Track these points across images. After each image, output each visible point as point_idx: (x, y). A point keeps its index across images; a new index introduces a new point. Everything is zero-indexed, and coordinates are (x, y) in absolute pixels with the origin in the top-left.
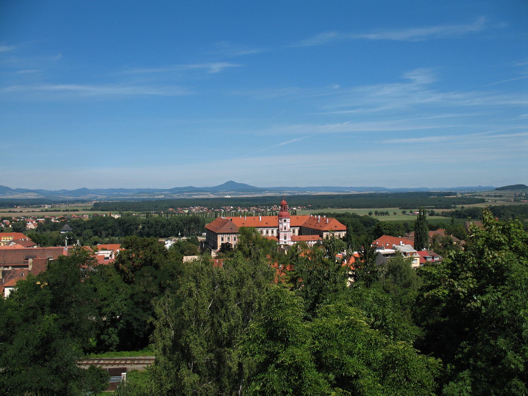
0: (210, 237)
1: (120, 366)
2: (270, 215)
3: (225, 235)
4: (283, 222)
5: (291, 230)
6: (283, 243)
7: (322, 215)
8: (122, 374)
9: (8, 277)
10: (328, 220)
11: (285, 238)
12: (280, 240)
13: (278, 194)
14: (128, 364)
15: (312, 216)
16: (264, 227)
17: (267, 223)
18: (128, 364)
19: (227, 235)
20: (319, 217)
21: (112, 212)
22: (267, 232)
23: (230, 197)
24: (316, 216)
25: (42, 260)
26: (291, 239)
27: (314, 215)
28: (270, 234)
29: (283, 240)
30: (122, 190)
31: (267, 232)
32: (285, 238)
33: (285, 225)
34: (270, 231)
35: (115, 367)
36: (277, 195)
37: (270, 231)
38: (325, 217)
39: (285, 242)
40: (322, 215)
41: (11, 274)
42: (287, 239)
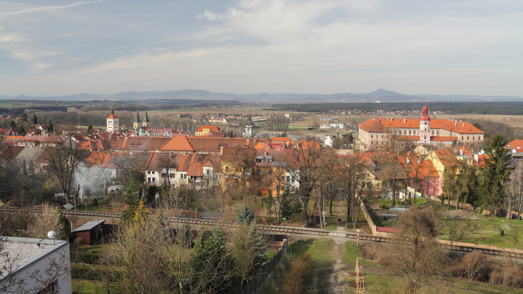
0: (362, 135)
1: (284, 234)
2: (413, 119)
5: (431, 131)
6: (424, 142)
7: (459, 120)
8: (284, 240)
9: (206, 159)
10: (463, 124)
11: (425, 138)
12: (420, 139)
13: (421, 101)
14: (289, 232)
16: (408, 128)
17: (410, 125)
18: (289, 232)
19: (376, 134)
20: (456, 121)
21: (285, 112)
22: (410, 132)
23: (380, 102)
24: (453, 121)
25: (230, 147)
27: (451, 119)
28: (412, 134)
29: (423, 139)
30: (294, 95)
31: (410, 132)
32: (425, 138)
34: (412, 132)
35: (279, 233)
36: (420, 102)
37: (412, 132)
38: (461, 121)
41: (208, 157)
42: (427, 139)
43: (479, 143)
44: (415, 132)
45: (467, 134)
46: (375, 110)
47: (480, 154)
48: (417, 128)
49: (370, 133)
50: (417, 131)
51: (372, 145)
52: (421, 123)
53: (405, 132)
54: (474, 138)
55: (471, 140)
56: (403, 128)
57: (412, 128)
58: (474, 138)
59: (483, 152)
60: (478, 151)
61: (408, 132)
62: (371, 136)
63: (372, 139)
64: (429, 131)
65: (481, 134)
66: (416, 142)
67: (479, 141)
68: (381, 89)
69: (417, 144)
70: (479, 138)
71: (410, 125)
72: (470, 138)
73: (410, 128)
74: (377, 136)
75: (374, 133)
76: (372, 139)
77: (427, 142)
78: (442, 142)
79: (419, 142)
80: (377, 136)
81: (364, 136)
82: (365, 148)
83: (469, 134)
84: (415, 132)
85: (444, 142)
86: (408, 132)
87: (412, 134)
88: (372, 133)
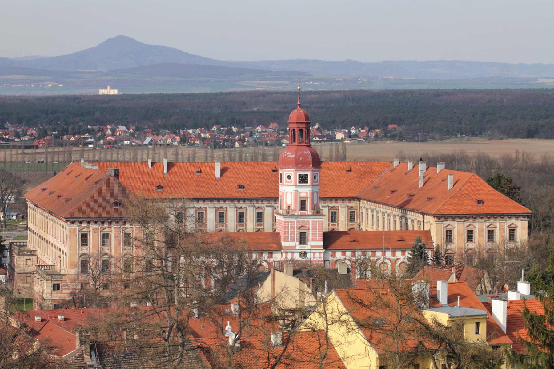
0: (42, 233)
2: (254, 159)
3: (96, 226)
4: (298, 184)
5: (325, 211)
6: (297, 256)
10: (450, 179)
11: (303, 239)
12: (283, 244)
15: (396, 163)
16: (232, 200)
17: (241, 187)
20: (422, 166)
22: (241, 218)
23: (114, 92)
24: (410, 165)
26: (321, 243)
27: (403, 159)
28: (250, 225)
29: (296, 244)
31: (241, 218)
32: (303, 239)
33: (303, 195)
38: (440, 167)
39: (304, 254)
40: (432, 162)
42: (310, 244)
43: (510, 252)
44: (259, 217)
45: (466, 217)
46: (96, 128)
47: (512, 296)
48: (268, 199)
49: (76, 226)
50: (267, 213)
51: (83, 277)
52: (285, 178)
53: (221, 217)
54: (491, 235)
55: (479, 244)
56: (211, 200)
57: (251, 200)
58: (491, 235)
59: (524, 288)
60: (507, 287)
61: (231, 215)
62: (78, 238)
63: (85, 250)
64: (317, 212)
65: (517, 216)
66: (265, 256)
67: (512, 245)
68: (121, 39)
69: (269, 264)
70: (512, 233)
71: (241, 187)
72: (476, 235)
73: (239, 200)
74: (106, 236)
75: (92, 226)
76: (85, 250)
77: (310, 256)
78: (370, 253)
79: (277, 256)
80: (106, 236)
81: (51, 239)
82: (56, 287)
83: (474, 217)
84: (259, 217)
85: (379, 254)
86: (231, 215)
87: (250, 225)
88: (84, 225)
